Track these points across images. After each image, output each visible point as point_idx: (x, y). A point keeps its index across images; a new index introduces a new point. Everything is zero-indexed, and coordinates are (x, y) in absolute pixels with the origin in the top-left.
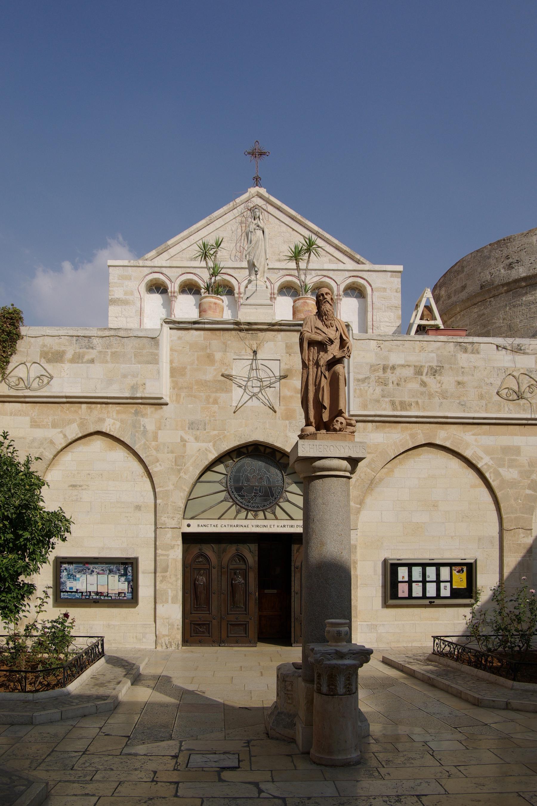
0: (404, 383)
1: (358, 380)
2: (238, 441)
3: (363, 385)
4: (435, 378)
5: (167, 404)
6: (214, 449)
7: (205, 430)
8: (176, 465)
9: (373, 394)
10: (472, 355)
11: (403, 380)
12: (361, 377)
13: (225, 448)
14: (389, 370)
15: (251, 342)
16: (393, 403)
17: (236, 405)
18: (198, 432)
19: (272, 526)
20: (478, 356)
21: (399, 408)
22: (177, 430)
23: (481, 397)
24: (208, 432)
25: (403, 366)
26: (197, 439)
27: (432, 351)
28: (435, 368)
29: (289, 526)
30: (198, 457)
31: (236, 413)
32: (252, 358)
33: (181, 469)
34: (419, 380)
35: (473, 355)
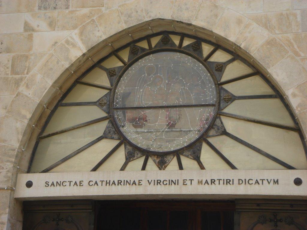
2: (126, 22)
6: (82, 40)
7: (67, 8)
8: (14, 72)
13: (101, 37)
18: (55, 13)
19: (188, 182)
22: (19, 11)
24: (72, 12)
26: (52, 25)
29: (221, 182)
30: (53, 55)
33: (21, 79)
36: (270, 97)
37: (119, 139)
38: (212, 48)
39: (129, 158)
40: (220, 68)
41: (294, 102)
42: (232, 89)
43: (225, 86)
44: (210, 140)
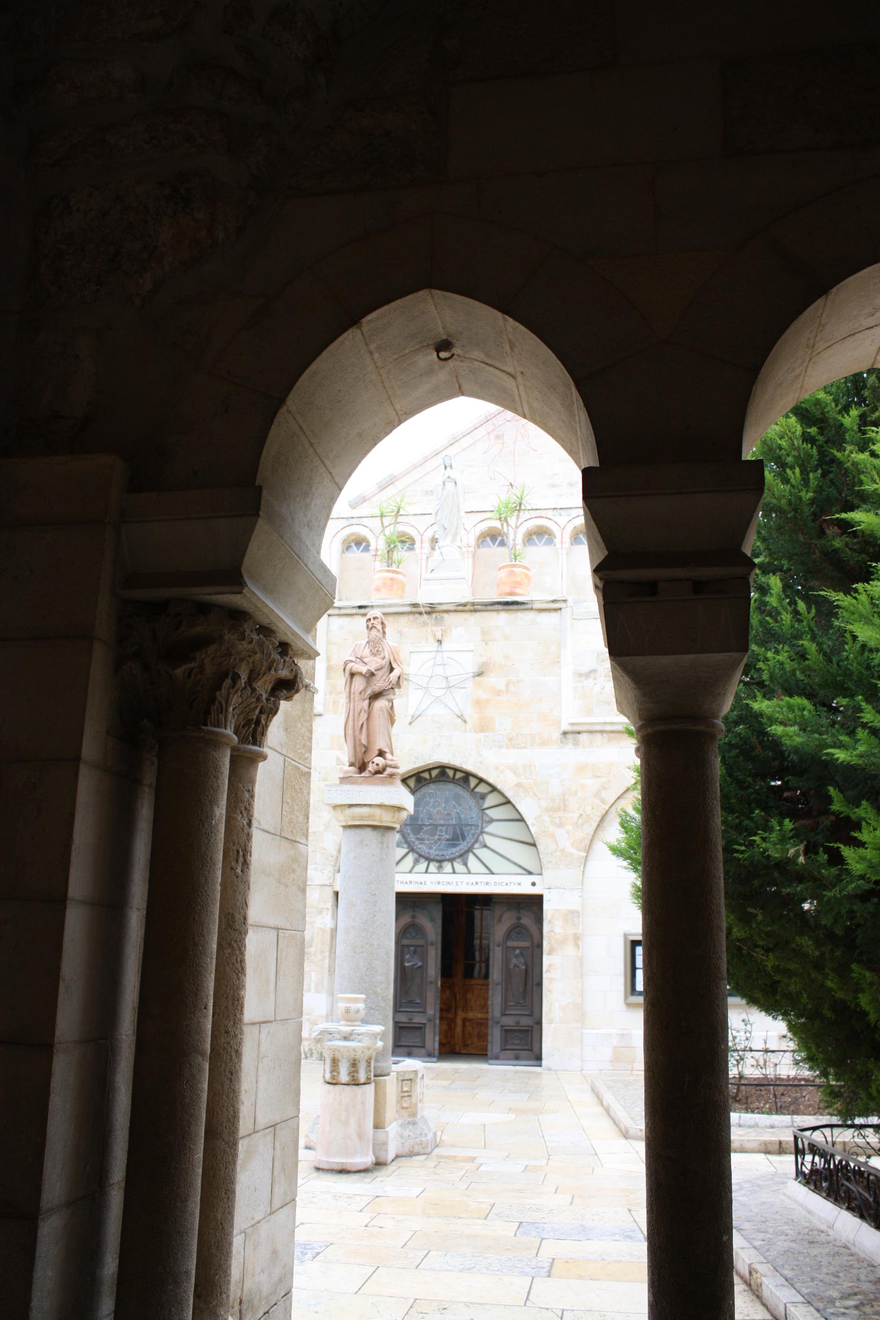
1: (581, 675)
2: (414, 763)
5: (320, 715)
12: (584, 669)
15: (434, 629)
17: (412, 713)
31: (413, 724)
32: (435, 649)
36: (518, 820)
37: (408, 848)
38: (476, 781)
39: (416, 862)
40: (483, 797)
41: (533, 830)
42: (492, 813)
43: (486, 811)
44: (475, 851)
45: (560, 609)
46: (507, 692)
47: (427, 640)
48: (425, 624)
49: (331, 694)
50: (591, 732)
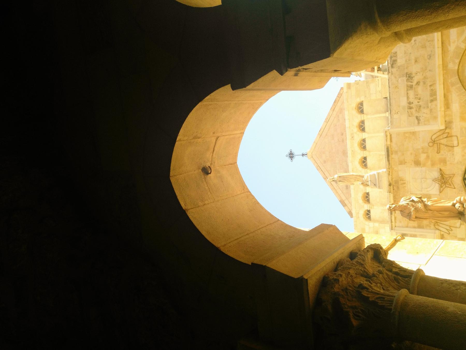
0: (418, 96)
1: (419, 123)
3: (422, 120)
4: (414, 77)
9: (427, 114)
10: (398, 57)
11: (417, 97)
14: (411, 105)
15: (400, 184)
16: (432, 101)
20: (398, 52)
21: (435, 97)
23: (424, 47)
25: (408, 98)
27: (397, 81)
28: (407, 78)
34: (416, 86)
35: (398, 55)
45: (390, 133)
46: (427, 153)
47: (405, 187)
48: (398, 188)
49: (430, 227)
50: (445, 116)
